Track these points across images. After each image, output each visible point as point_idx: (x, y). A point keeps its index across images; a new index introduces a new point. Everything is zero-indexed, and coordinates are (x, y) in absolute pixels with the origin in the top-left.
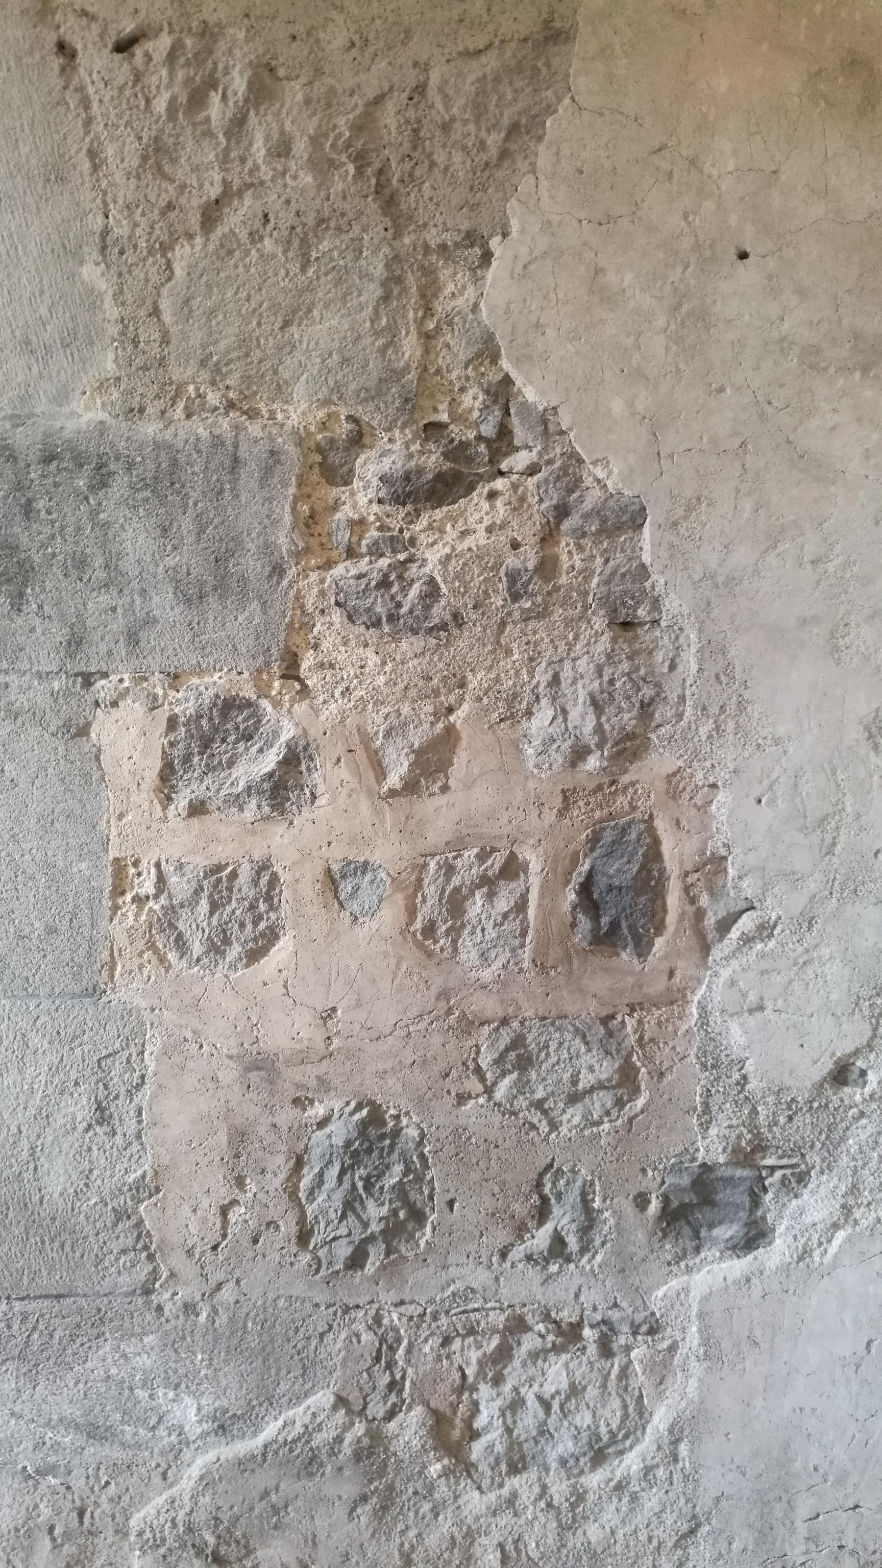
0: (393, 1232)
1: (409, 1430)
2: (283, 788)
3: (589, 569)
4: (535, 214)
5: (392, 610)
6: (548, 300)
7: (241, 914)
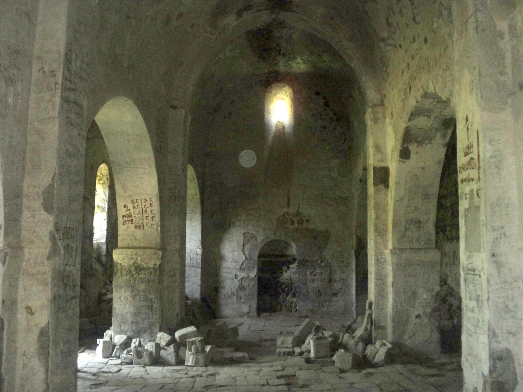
0: (321, 295)
1: (321, 305)
2: (315, 275)
3: (329, 265)
4: (327, 250)
7: (313, 281)
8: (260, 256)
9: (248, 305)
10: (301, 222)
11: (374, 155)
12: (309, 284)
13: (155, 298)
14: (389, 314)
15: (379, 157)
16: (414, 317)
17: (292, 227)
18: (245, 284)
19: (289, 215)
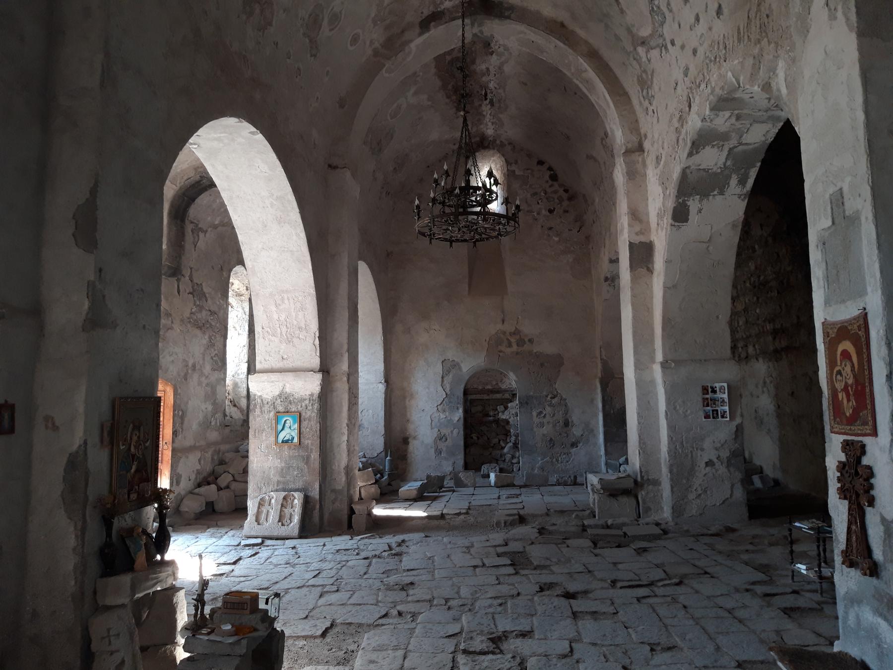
2: (544, 417)
3: (563, 403)
5: (550, 405)
6: (559, 386)
7: (542, 425)
8: (466, 393)
9: (451, 463)
10: (521, 343)
11: (629, 225)
12: (535, 429)
13: (312, 444)
14: (662, 461)
15: (637, 228)
16: (703, 465)
17: (509, 350)
18: (445, 431)
19: (504, 333)
